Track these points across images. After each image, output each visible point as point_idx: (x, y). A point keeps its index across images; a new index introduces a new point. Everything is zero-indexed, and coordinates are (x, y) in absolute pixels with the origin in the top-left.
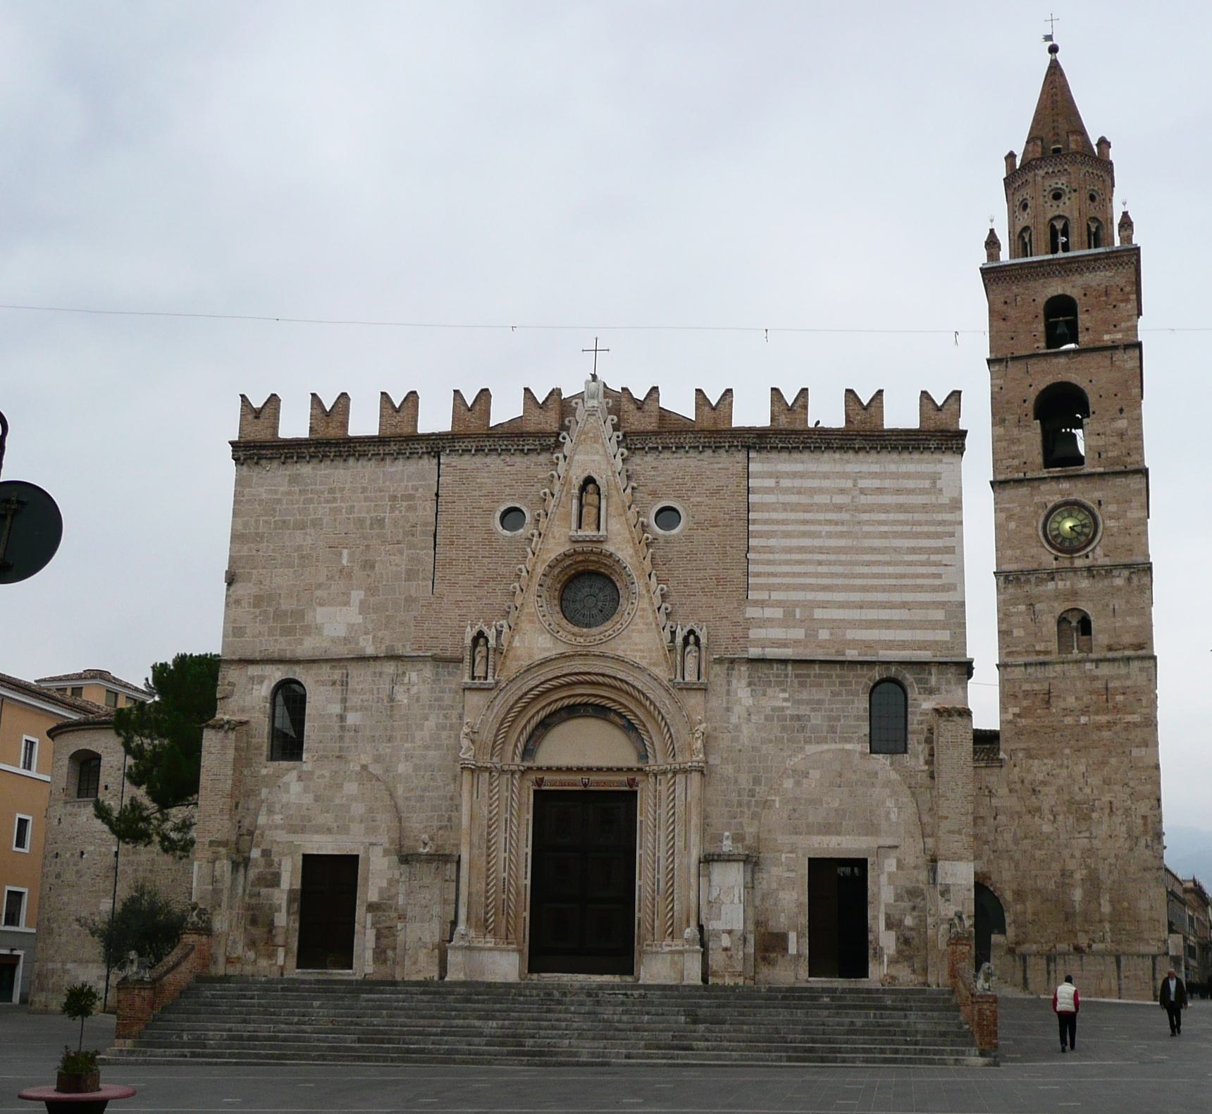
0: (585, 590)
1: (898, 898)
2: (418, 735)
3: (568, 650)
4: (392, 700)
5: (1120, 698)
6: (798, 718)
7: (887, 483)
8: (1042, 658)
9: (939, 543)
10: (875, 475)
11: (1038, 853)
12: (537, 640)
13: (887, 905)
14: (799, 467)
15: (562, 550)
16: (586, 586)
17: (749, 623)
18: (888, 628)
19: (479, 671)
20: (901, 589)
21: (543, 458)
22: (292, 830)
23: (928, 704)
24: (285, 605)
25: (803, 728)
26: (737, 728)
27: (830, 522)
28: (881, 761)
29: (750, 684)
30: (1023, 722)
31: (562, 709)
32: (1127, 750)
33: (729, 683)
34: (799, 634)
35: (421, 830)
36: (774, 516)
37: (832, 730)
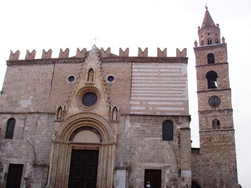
0: (88, 97)
1: (170, 181)
2: (42, 133)
3: (83, 112)
4: (36, 124)
6: (143, 130)
7: (168, 70)
8: (209, 130)
9: (182, 85)
10: (164, 68)
11: (209, 175)
12: (75, 109)
13: (167, 183)
14: (145, 67)
15: (83, 86)
16: (89, 96)
17: (131, 105)
18: (168, 107)
19: (59, 117)
20: (172, 97)
21: (80, 64)
22: (8, 157)
23: (178, 127)
24: (14, 99)
25: (144, 133)
26: (127, 133)
27: (153, 80)
28: (166, 143)
29: (130, 121)
30: (205, 145)
31: (81, 127)
33: (125, 121)
34: (144, 108)
35: (40, 158)
36: (138, 78)
37: (152, 134)
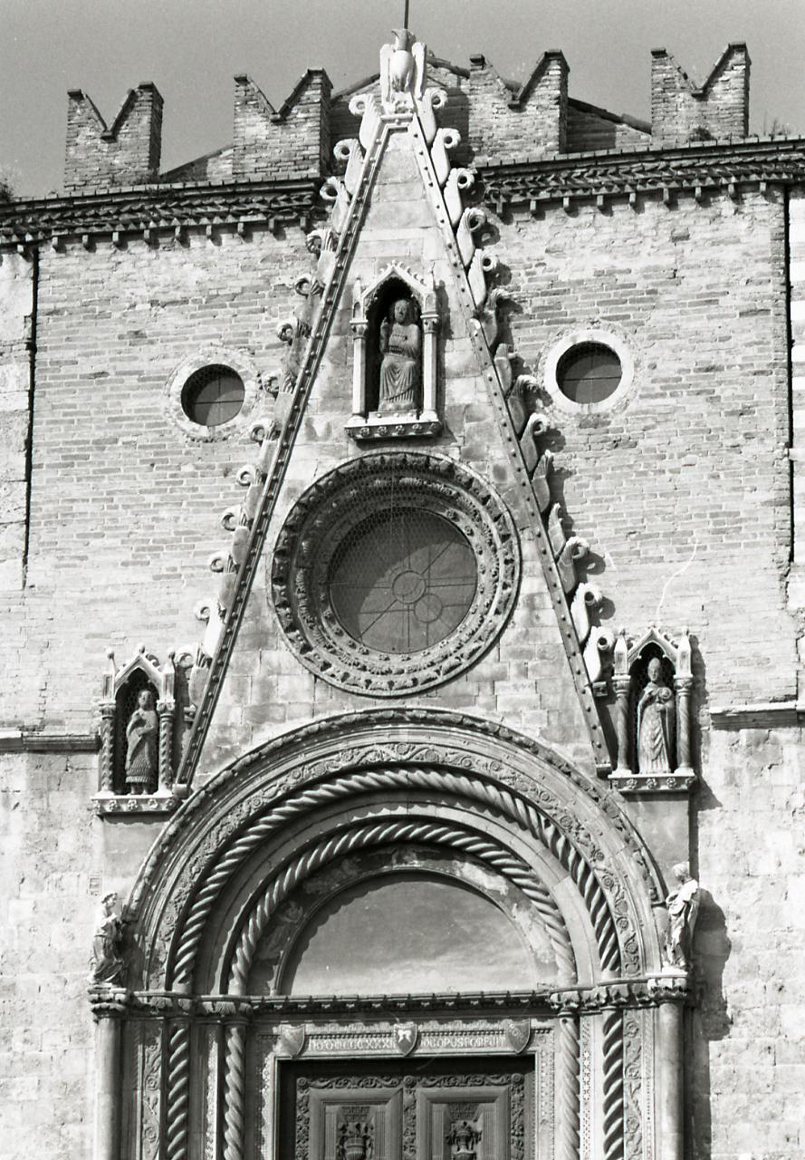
3: (350, 709)
15: (333, 463)
31: (346, 853)
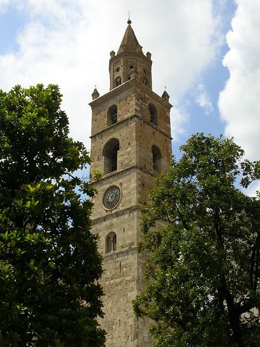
5: (125, 269)
32: (126, 294)
